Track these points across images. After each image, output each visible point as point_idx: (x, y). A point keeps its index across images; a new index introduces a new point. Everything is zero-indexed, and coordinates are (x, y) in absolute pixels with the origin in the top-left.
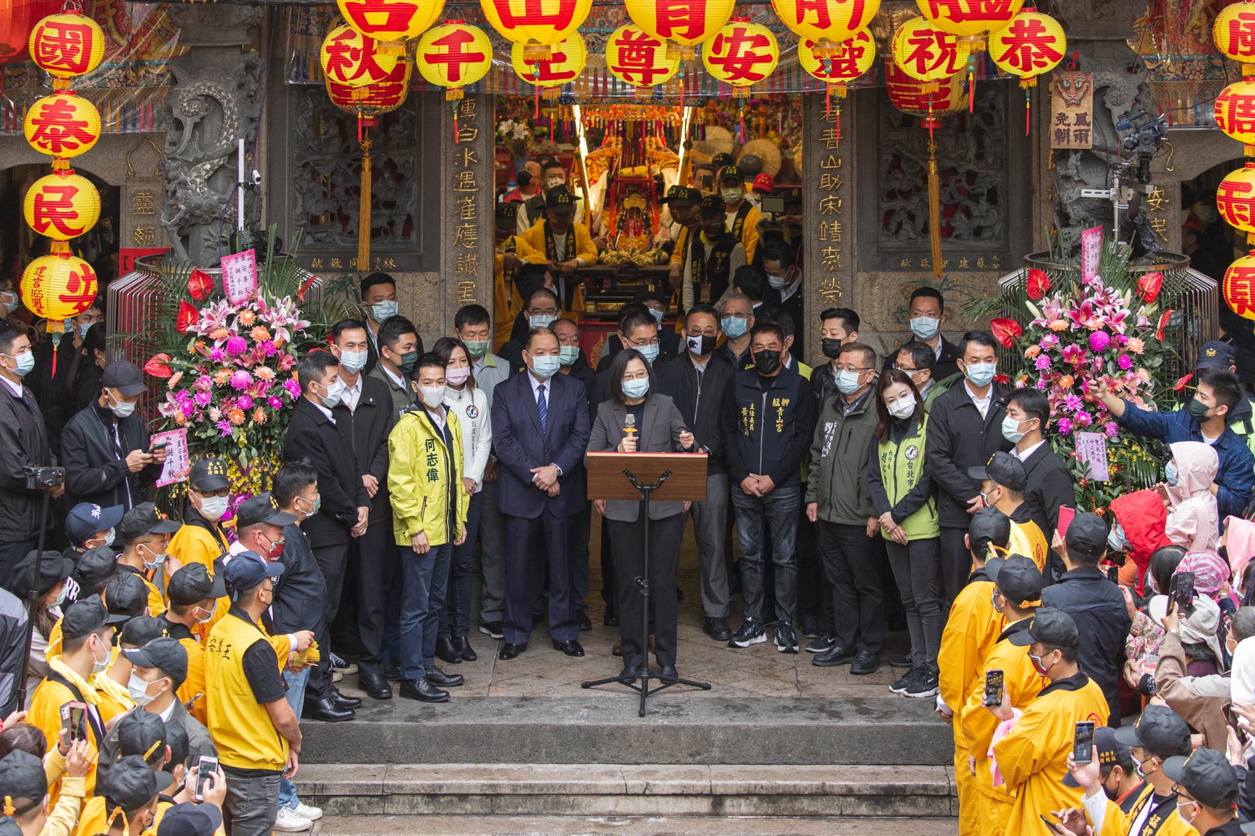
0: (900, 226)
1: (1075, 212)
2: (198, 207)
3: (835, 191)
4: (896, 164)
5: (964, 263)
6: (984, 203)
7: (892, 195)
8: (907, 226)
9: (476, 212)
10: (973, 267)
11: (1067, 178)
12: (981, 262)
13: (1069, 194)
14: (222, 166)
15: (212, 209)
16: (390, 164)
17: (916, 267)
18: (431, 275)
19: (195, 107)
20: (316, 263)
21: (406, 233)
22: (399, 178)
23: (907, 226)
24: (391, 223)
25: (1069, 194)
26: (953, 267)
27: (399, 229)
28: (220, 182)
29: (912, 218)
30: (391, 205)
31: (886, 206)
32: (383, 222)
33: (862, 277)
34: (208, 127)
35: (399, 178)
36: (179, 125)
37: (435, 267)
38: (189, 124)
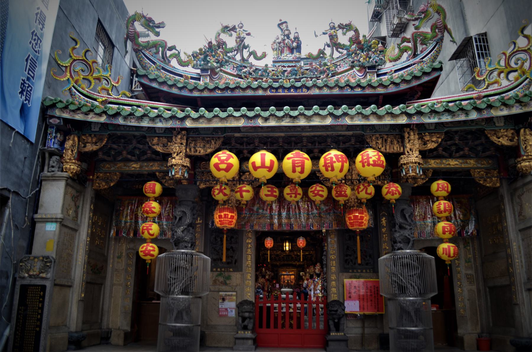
0: (349, 262)
1: (398, 239)
2: (179, 237)
3: (334, 254)
4: (348, 248)
5: (364, 271)
6: (368, 258)
7: (347, 256)
8: (351, 263)
9: (251, 258)
10: (366, 272)
11: (396, 231)
12: (368, 271)
13: (397, 235)
14: (186, 228)
15: (183, 238)
16: (232, 248)
17: (353, 272)
18: (240, 273)
19: (179, 213)
20: (215, 269)
21: (235, 263)
22: (233, 251)
23: (351, 263)
24: (232, 261)
25: (397, 235)
26: (362, 272)
27: (234, 262)
28: (185, 232)
29: (352, 261)
30: (232, 257)
31: (346, 258)
32: (230, 261)
33: (341, 274)
34: (183, 220)
35: (233, 251)
36: (176, 218)
37: (241, 271)
38: (178, 218)
